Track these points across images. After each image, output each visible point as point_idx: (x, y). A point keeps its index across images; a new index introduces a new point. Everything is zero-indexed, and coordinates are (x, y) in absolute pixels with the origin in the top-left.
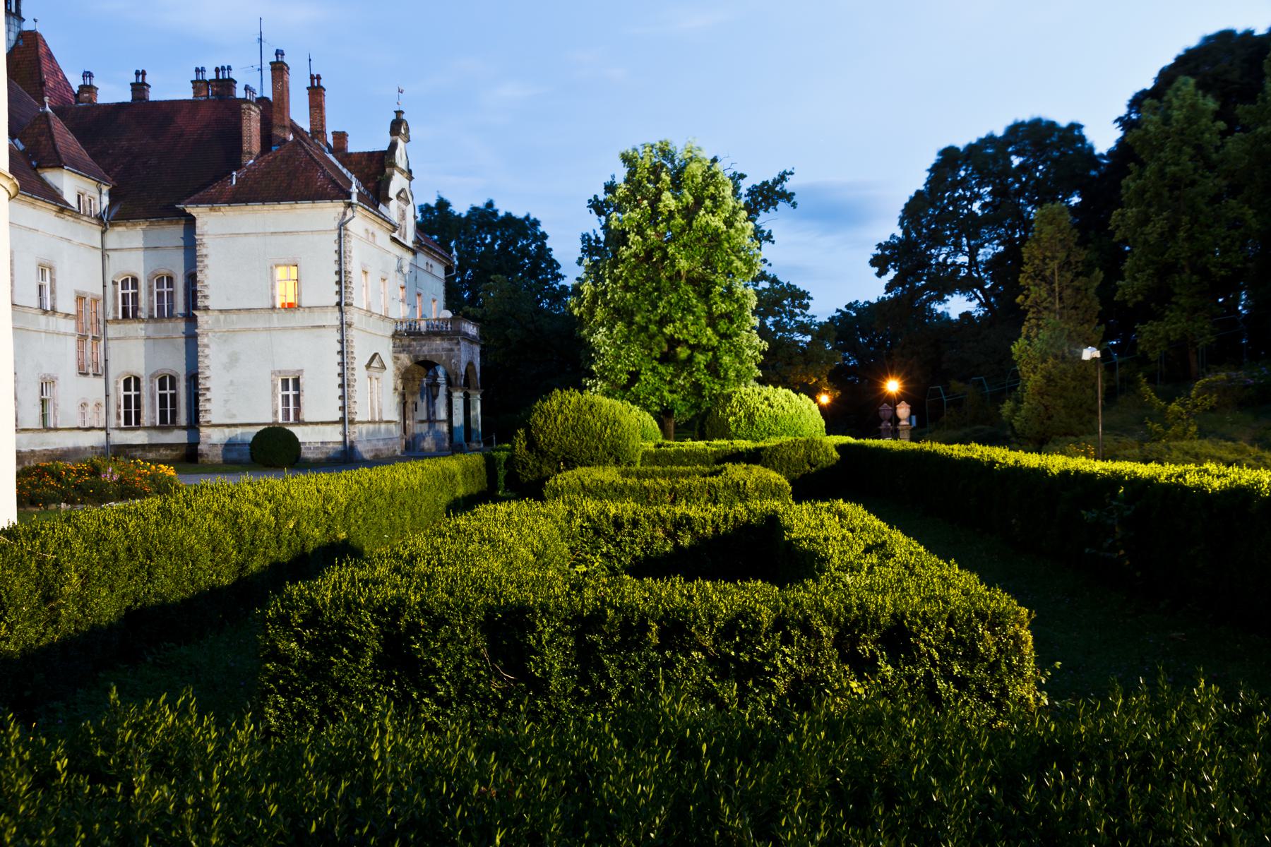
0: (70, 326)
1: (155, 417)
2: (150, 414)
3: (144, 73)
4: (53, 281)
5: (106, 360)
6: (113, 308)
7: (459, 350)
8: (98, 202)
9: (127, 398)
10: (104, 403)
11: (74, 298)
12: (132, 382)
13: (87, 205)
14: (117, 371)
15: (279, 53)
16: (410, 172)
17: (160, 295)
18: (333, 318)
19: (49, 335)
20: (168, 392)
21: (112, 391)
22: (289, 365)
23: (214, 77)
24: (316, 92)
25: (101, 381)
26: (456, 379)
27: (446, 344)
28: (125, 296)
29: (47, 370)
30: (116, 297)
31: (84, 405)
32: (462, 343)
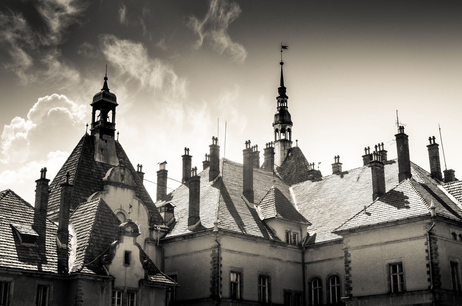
3: (338, 157)
4: (269, 284)
8: (299, 235)
13: (292, 238)
15: (402, 128)
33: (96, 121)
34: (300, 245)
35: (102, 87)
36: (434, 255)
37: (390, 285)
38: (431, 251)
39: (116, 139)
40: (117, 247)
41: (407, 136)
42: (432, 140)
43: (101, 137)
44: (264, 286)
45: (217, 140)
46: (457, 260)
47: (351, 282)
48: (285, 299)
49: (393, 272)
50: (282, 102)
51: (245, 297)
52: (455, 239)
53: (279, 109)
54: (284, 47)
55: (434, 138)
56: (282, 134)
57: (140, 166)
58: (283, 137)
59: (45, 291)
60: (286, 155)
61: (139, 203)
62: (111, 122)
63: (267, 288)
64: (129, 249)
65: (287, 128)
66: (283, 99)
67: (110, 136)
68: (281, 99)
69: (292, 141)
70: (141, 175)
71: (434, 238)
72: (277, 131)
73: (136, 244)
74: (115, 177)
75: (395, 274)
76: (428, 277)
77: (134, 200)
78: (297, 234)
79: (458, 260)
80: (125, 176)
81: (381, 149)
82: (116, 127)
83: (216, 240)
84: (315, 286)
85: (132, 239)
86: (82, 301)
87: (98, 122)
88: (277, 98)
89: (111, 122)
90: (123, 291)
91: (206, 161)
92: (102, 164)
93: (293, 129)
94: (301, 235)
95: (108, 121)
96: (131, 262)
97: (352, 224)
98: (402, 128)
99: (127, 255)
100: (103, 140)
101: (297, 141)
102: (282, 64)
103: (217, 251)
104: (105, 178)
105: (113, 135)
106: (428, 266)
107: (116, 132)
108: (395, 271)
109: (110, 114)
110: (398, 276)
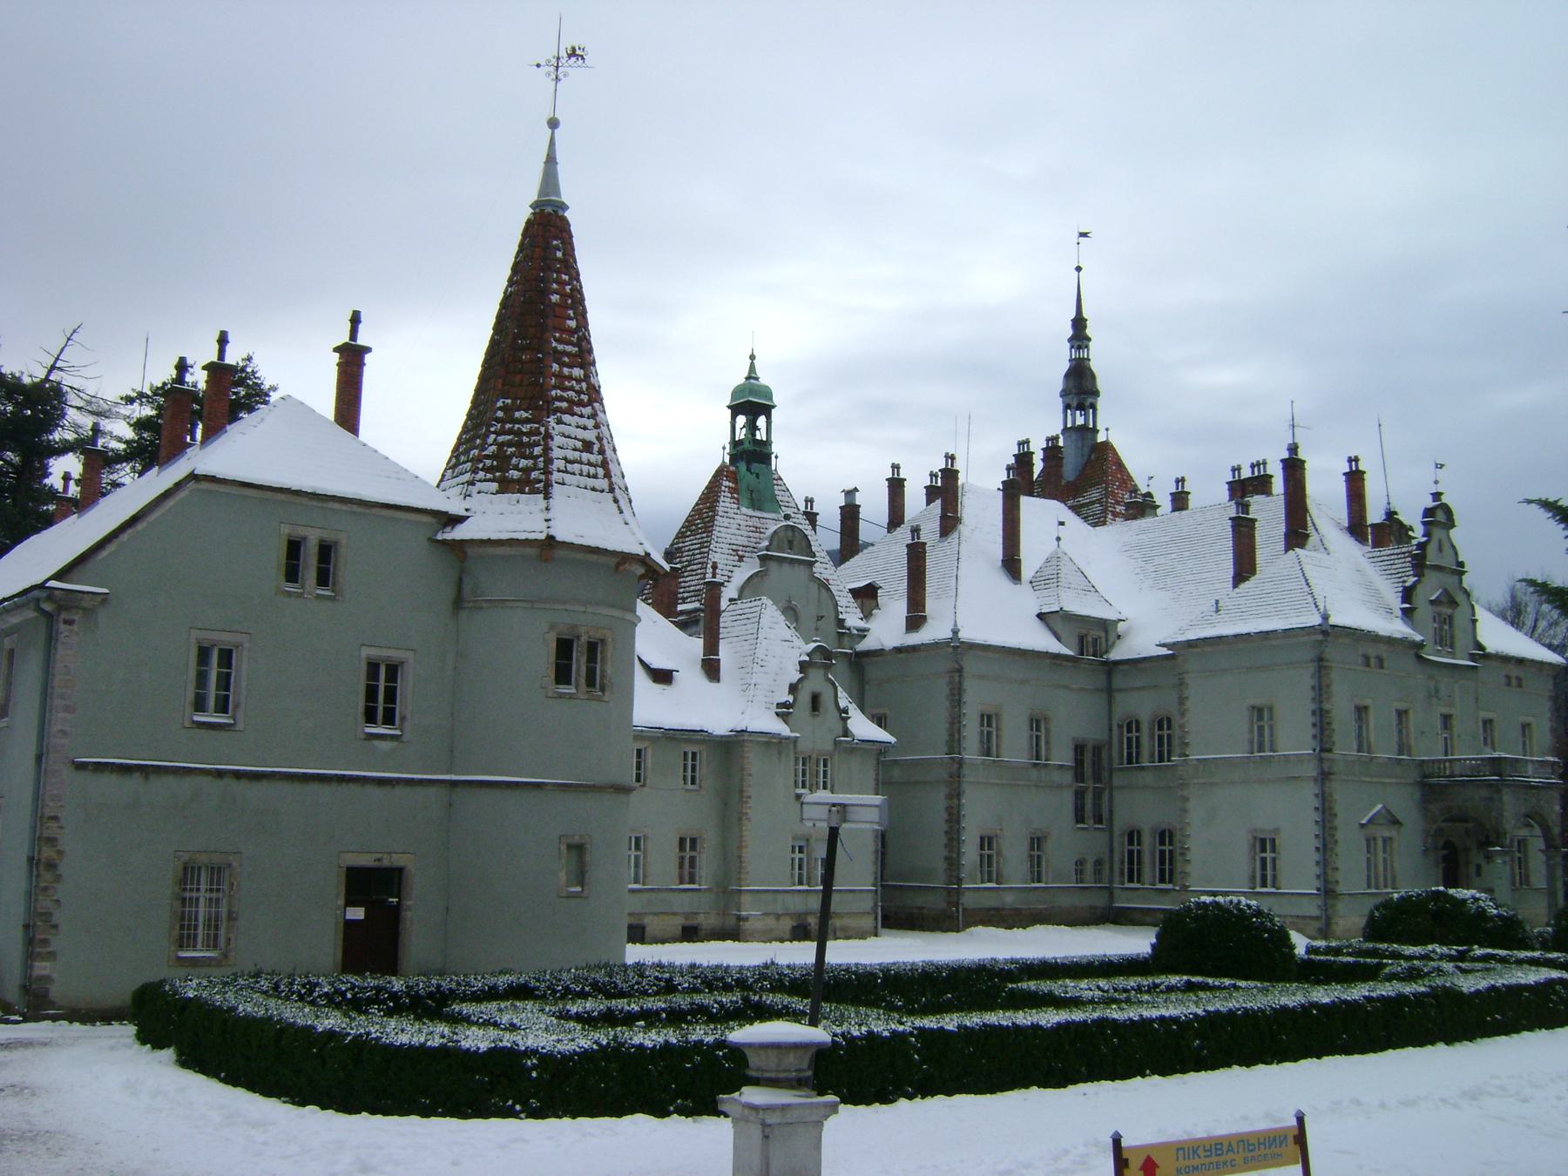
0: (1068, 777)
3: (1183, 480)
4: (1047, 730)
5: (1111, 812)
7: (1500, 800)
8: (1103, 640)
9: (1131, 853)
10: (1106, 858)
11: (1071, 746)
12: (1133, 836)
13: (1090, 645)
14: (1121, 822)
15: (1293, 449)
16: (1461, 564)
17: (1161, 738)
18: (1311, 770)
20: (1167, 848)
21: (1116, 845)
22: (1264, 823)
23: (1250, 475)
24: (1355, 479)
27: (1484, 793)
28: (1129, 740)
30: (1121, 742)
31: (1080, 863)
32: (1505, 790)
33: (737, 439)
35: (746, 374)
36: (1325, 696)
38: (1320, 689)
39: (773, 468)
40: (800, 686)
41: (1303, 462)
42: (1353, 463)
43: (749, 470)
44: (1038, 733)
45: (952, 458)
46: (1368, 702)
48: (1076, 754)
49: (1258, 720)
50: (1079, 348)
52: (1368, 665)
53: (1074, 363)
54: (1083, 235)
55: (1356, 460)
56: (1078, 412)
57: (810, 501)
58: (1080, 421)
59: (694, 759)
60: (1086, 458)
61: (819, 588)
62: (764, 439)
63: (1043, 737)
65: (1087, 404)
66: (1080, 343)
67: (764, 466)
68: (1077, 344)
69: (1098, 428)
71: (1325, 667)
72: (1067, 407)
75: (1262, 723)
77: (812, 583)
78: (1100, 638)
79: (1370, 700)
80: (795, 543)
81: (1262, 473)
82: (775, 448)
83: (956, 661)
84: (1129, 731)
85: (822, 672)
86: (750, 775)
87: (741, 442)
89: (764, 439)
90: (810, 757)
93: (1101, 403)
94: (1107, 640)
95: (758, 437)
97: (1191, 636)
98: (1293, 449)
100: (751, 473)
101: (1107, 429)
102: (1079, 269)
103: (957, 679)
105: (770, 464)
106: (1314, 713)
107: (773, 456)
108: (1260, 718)
109: (761, 422)
110: (1266, 727)
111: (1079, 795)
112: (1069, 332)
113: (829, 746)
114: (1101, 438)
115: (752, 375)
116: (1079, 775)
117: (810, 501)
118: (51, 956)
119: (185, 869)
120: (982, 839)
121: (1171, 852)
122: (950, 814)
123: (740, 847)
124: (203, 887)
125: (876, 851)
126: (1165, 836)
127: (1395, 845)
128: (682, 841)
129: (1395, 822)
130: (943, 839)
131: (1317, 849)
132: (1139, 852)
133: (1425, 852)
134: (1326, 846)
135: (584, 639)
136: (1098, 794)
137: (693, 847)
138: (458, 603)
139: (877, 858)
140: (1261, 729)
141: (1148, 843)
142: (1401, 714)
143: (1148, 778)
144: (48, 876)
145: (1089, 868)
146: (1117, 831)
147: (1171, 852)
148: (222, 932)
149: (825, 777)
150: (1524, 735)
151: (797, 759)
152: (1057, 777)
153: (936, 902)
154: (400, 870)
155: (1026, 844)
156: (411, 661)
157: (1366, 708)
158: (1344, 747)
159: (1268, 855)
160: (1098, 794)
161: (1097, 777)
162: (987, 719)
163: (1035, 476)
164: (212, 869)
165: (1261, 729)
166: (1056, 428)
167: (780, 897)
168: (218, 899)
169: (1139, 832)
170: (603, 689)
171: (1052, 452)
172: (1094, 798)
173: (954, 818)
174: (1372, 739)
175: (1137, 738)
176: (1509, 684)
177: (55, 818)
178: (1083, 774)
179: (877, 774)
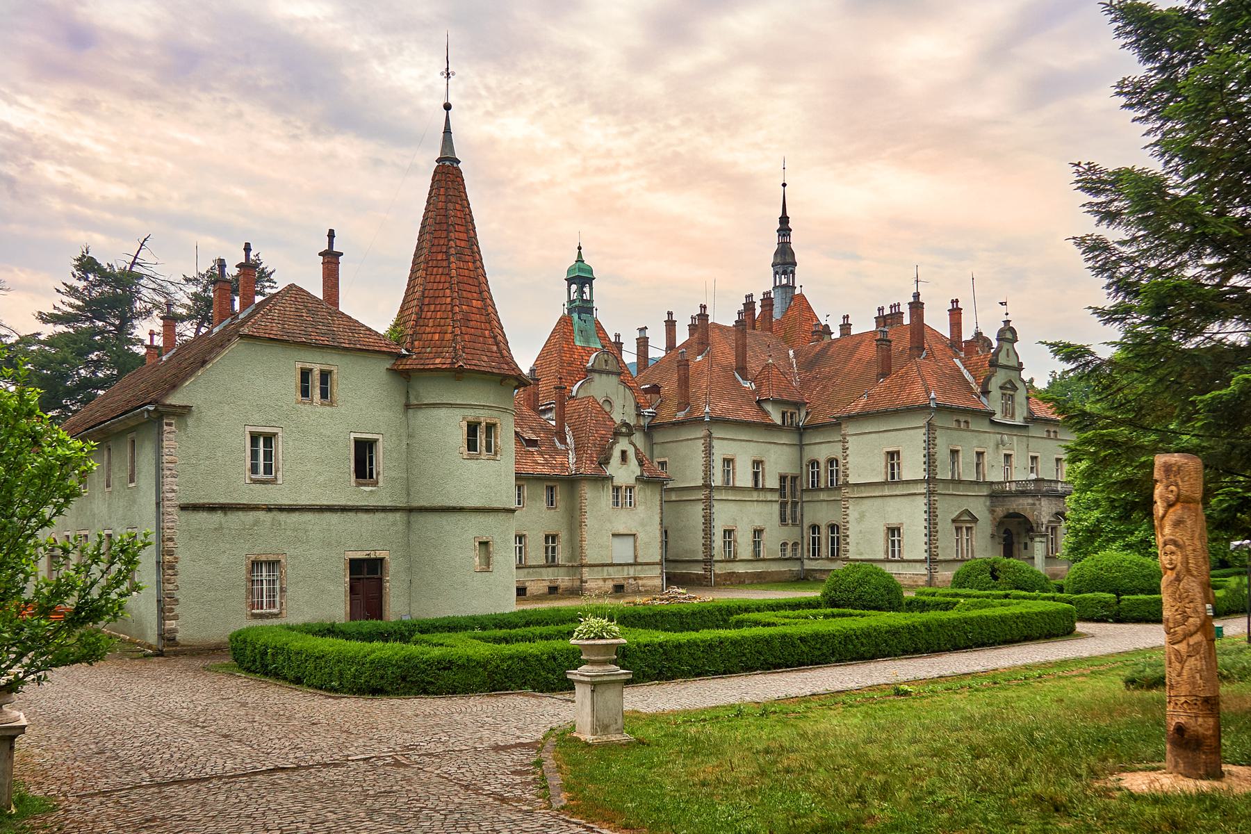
0: (776, 497)
1: (828, 552)
2: (825, 551)
4: (763, 469)
5: (802, 515)
6: (806, 482)
7: (1040, 504)
10: (800, 542)
11: (778, 477)
12: (815, 528)
18: (922, 489)
19: (760, 503)
21: (805, 535)
22: (893, 522)
25: (797, 529)
26: (1037, 527)
27: (1030, 501)
28: (813, 473)
29: (758, 524)
31: (785, 544)
32: (1043, 499)
34: (798, 427)
37: (887, 474)
43: (579, 318)
45: (705, 307)
46: (958, 448)
47: (848, 469)
50: (784, 235)
51: (738, 484)
58: (784, 281)
64: (625, 449)
65: (789, 271)
68: (782, 233)
70: (619, 345)
72: (776, 273)
73: (632, 443)
74: (599, 364)
76: (924, 466)
84: (813, 468)
87: (574, 301)
88: (778, 231)
90: (621, 487)
91: (692, 324)
92: (583, 348)
93: (797, 270)
95: (585, 298)
96: (628, 461)
99: (624, 453)
101: (801, 286)
104: (590, 364)
106: (925, 456)
108: (893, 459)
109: (587, 290)
111: (783, 505)
112: (778, 226)
113: (632, 482)
114: (797, 291)
115: (580, 260)
116: (783, 495)
117: (618, 336)
118: (176, 618)
119: (253, 564)
120: (725, 531)
121: (838, 537)
122: (706, 520)
123: (582, 541)
124: (264, 574)
125: (662, 542)
126: (833, 527)
127: (974, 532)
128: (547, 537)
129: (975, 520)
130: (702, 534)
131: (926, 535)
132: (819, 538)
133: (993, 536)
134: (932, 532)
135: (484, 424)
136: (795, 504)
137: (553, 542)
138: (408, 406)
139: (662, 545)
140: (892, 465)
141: (824, 533)
142: (980, 454)
143: (823, 496)
144: (170, 572)
145: (789, 547)
146: (805, 527)
147: (838, 537)
148: (277, 599)
149: (630, 499)
150: (1057, 466)
151: (613, 489)
152: (770, 497)
153: (698, 570)
154: (382, 560)
155: (751, 535)
156: (381, 440)
157: (957, 451)
158: (944, 473)
159: (896, 538)
160: (795, 504)
161: (793, 495)
162: (728, 462)
163: (756, 316)
164: (269, 564)
165: (892, 465)
166: (770, 287)
167: (605, 568)
168: (274, 580)
169: (819, 527)
170: (496, 454)
171: (767, 301)
172: (791, 508)
173: (708, 521)
174: (961, 471)
175: (818, 472)
176: (1049, 436)
177: (171, 539)
178: (785, 493)
179: (662, 498)
